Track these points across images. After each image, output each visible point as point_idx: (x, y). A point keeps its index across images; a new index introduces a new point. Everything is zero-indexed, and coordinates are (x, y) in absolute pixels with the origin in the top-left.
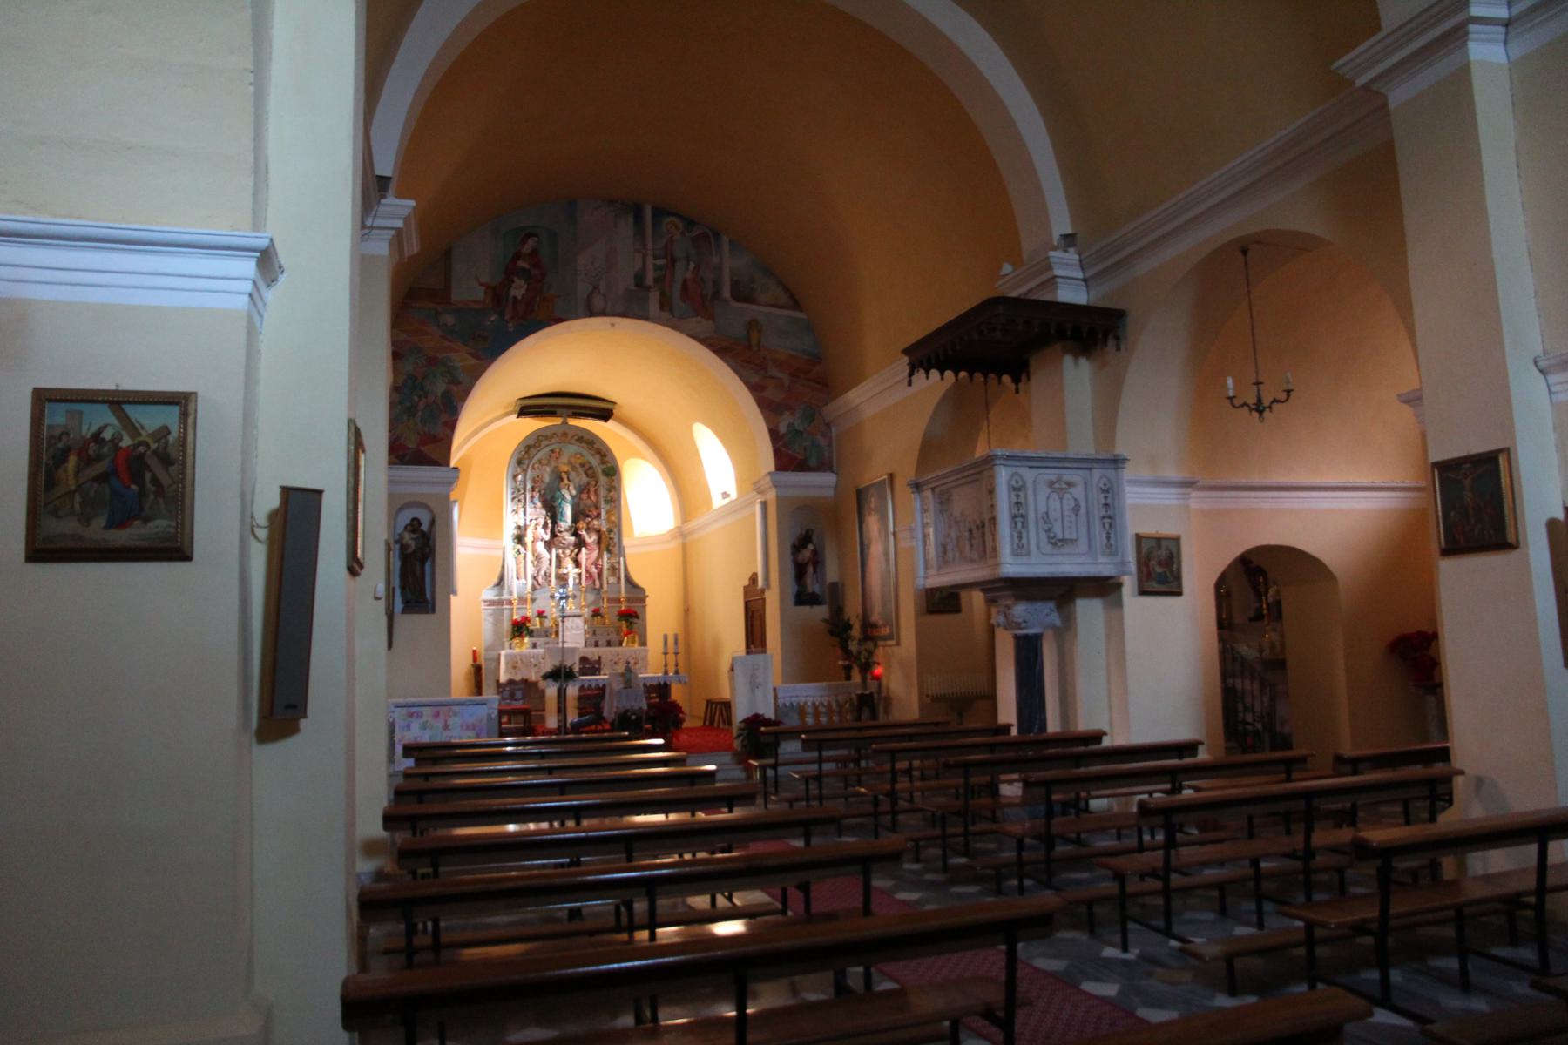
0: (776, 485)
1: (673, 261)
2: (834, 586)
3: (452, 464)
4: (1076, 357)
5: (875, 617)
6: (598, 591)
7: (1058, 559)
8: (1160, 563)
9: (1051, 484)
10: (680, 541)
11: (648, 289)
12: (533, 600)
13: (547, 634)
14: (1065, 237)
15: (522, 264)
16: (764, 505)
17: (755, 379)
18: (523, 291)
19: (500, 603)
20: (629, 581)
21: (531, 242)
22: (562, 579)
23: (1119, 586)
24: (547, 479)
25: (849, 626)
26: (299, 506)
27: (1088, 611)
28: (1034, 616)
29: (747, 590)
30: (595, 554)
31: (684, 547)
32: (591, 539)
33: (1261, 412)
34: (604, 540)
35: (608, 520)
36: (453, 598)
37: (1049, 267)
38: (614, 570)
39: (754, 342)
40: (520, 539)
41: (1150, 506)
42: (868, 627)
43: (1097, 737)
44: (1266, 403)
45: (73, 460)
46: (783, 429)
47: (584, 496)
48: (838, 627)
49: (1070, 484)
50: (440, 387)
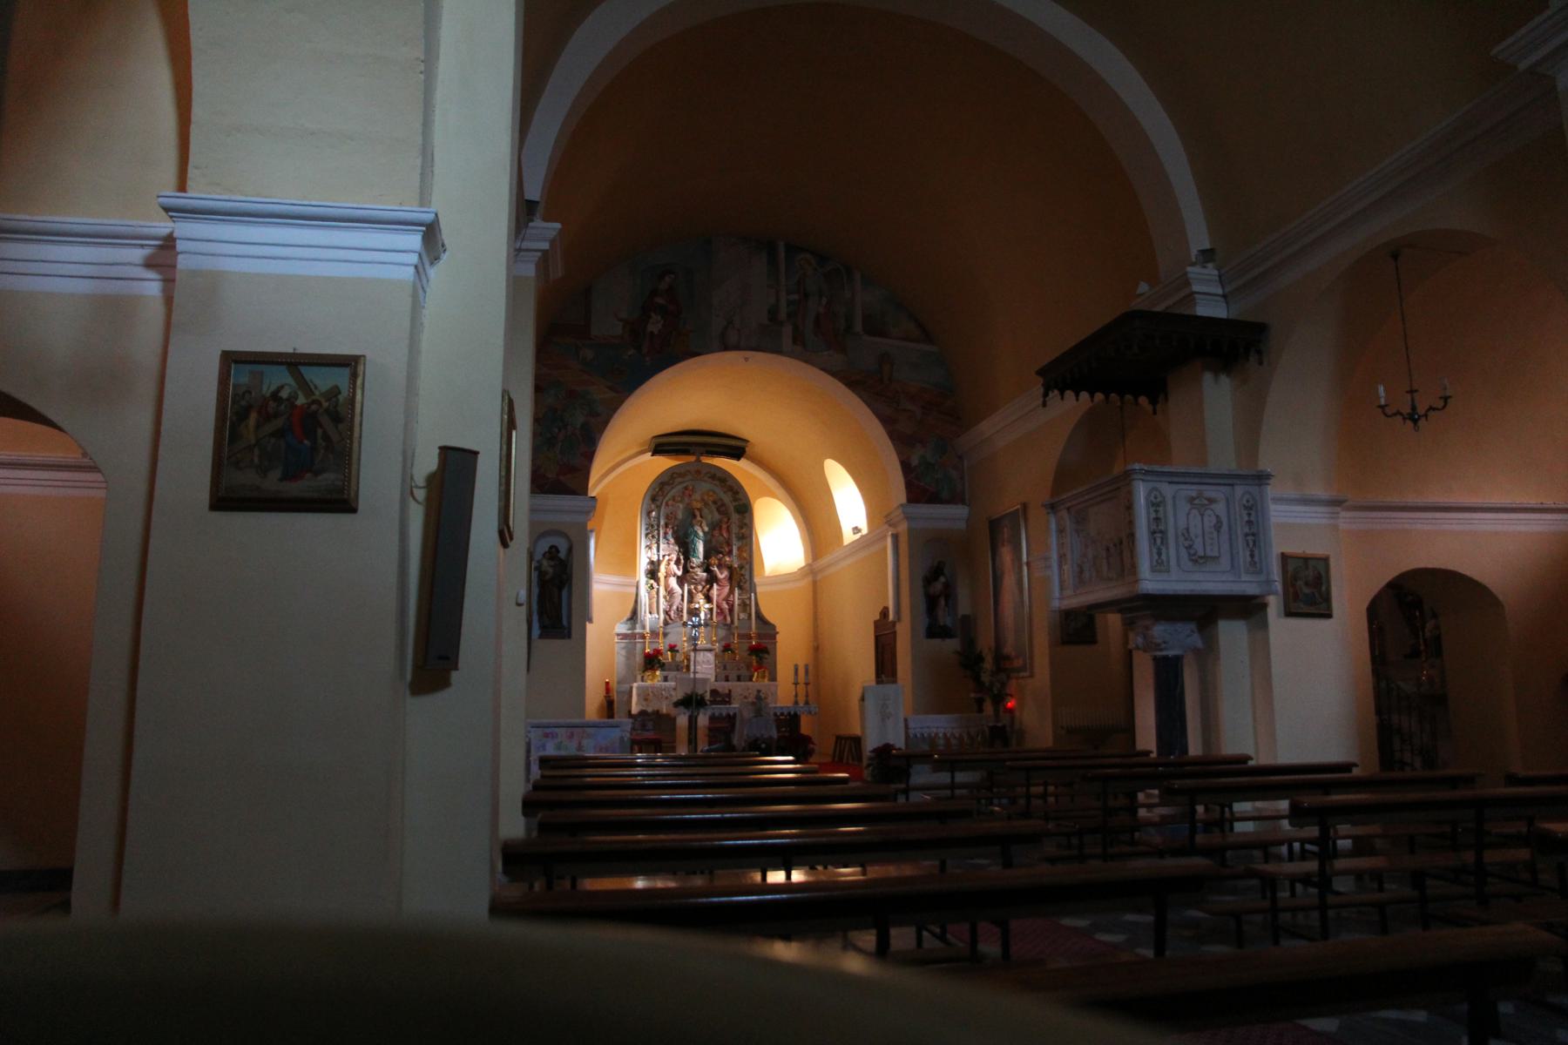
0: (908, 518)
2: (966, 619)
3: (592, 493)
4: (1216, 372)
5: (1008, 649)
6: (729, 627)
7: (1197, 577)
8: (1307, 584)
9: (1191, 500)
10: (810, 578)
12: (665, 635)
13: (678, 668)
14: (1203, 252)
15: (659, 300)
16: (895, 537)
19: (633, 636)
20: (759, 616)
22: (694, 613)
23: (1264, 606)
24: (680, 516)
25: (980, 659)
26: (457, 465)
27: (1232, 633)
28: (1175, 637)
29: (877, 624)
30: (727, 589)
31: (815, 583)
32: (722, 575)
33: (1415, 422)
34: (736, 577)
35: (739, 556)
36: (589, 626)
37: (1187, 283)
38: (745, 606)
40: (653, 573)
41: (1297, 523)
42: (1001, 659)
43: (1244, 759)
44: (1421, 410)
45: (253, 416)
46: (915, 461)
47: (716, 533)
48: (970, 660)
49: (1211, 501)
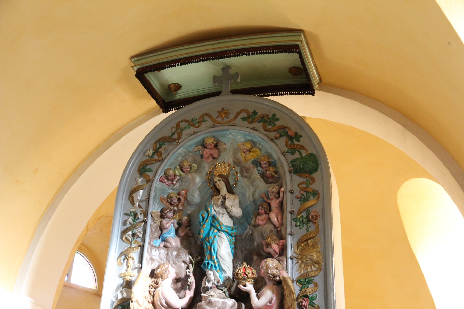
24: (196, 197)
35: (301, 258)
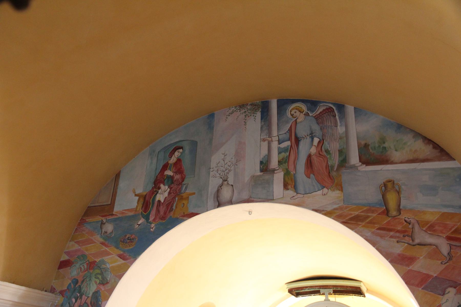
1: (297, 140)
11: (273, 171)
15: (169, 173)
17: (398, 249)
18: (166, 194)
21: (177, 154)
39: (392, 204)
50: (93, 288)
